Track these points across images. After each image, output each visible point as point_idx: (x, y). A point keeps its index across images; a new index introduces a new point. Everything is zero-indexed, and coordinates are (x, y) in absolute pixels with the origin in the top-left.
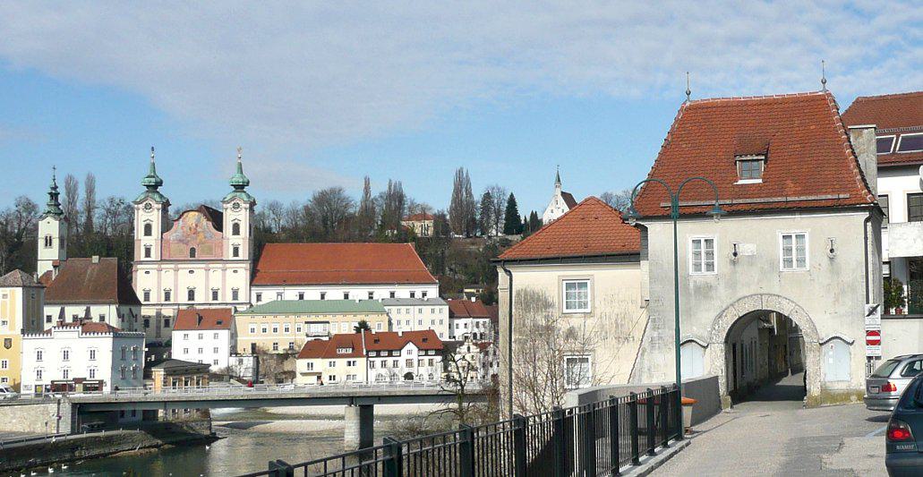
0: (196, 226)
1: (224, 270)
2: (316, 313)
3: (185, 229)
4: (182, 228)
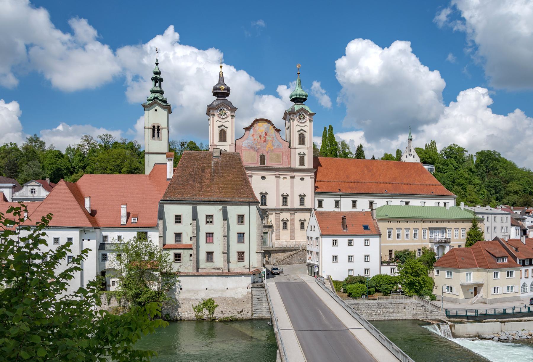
0: (266, 134)
1: (293, 177)
2: (437, 220)
3: (256, 137)
4: (253, 135)
